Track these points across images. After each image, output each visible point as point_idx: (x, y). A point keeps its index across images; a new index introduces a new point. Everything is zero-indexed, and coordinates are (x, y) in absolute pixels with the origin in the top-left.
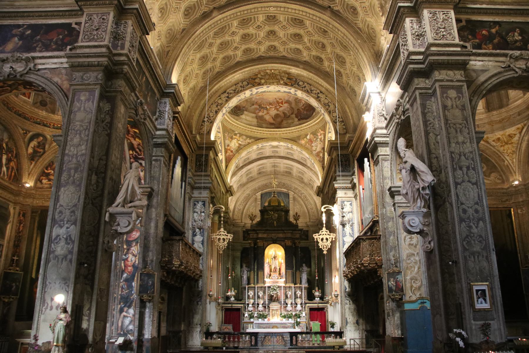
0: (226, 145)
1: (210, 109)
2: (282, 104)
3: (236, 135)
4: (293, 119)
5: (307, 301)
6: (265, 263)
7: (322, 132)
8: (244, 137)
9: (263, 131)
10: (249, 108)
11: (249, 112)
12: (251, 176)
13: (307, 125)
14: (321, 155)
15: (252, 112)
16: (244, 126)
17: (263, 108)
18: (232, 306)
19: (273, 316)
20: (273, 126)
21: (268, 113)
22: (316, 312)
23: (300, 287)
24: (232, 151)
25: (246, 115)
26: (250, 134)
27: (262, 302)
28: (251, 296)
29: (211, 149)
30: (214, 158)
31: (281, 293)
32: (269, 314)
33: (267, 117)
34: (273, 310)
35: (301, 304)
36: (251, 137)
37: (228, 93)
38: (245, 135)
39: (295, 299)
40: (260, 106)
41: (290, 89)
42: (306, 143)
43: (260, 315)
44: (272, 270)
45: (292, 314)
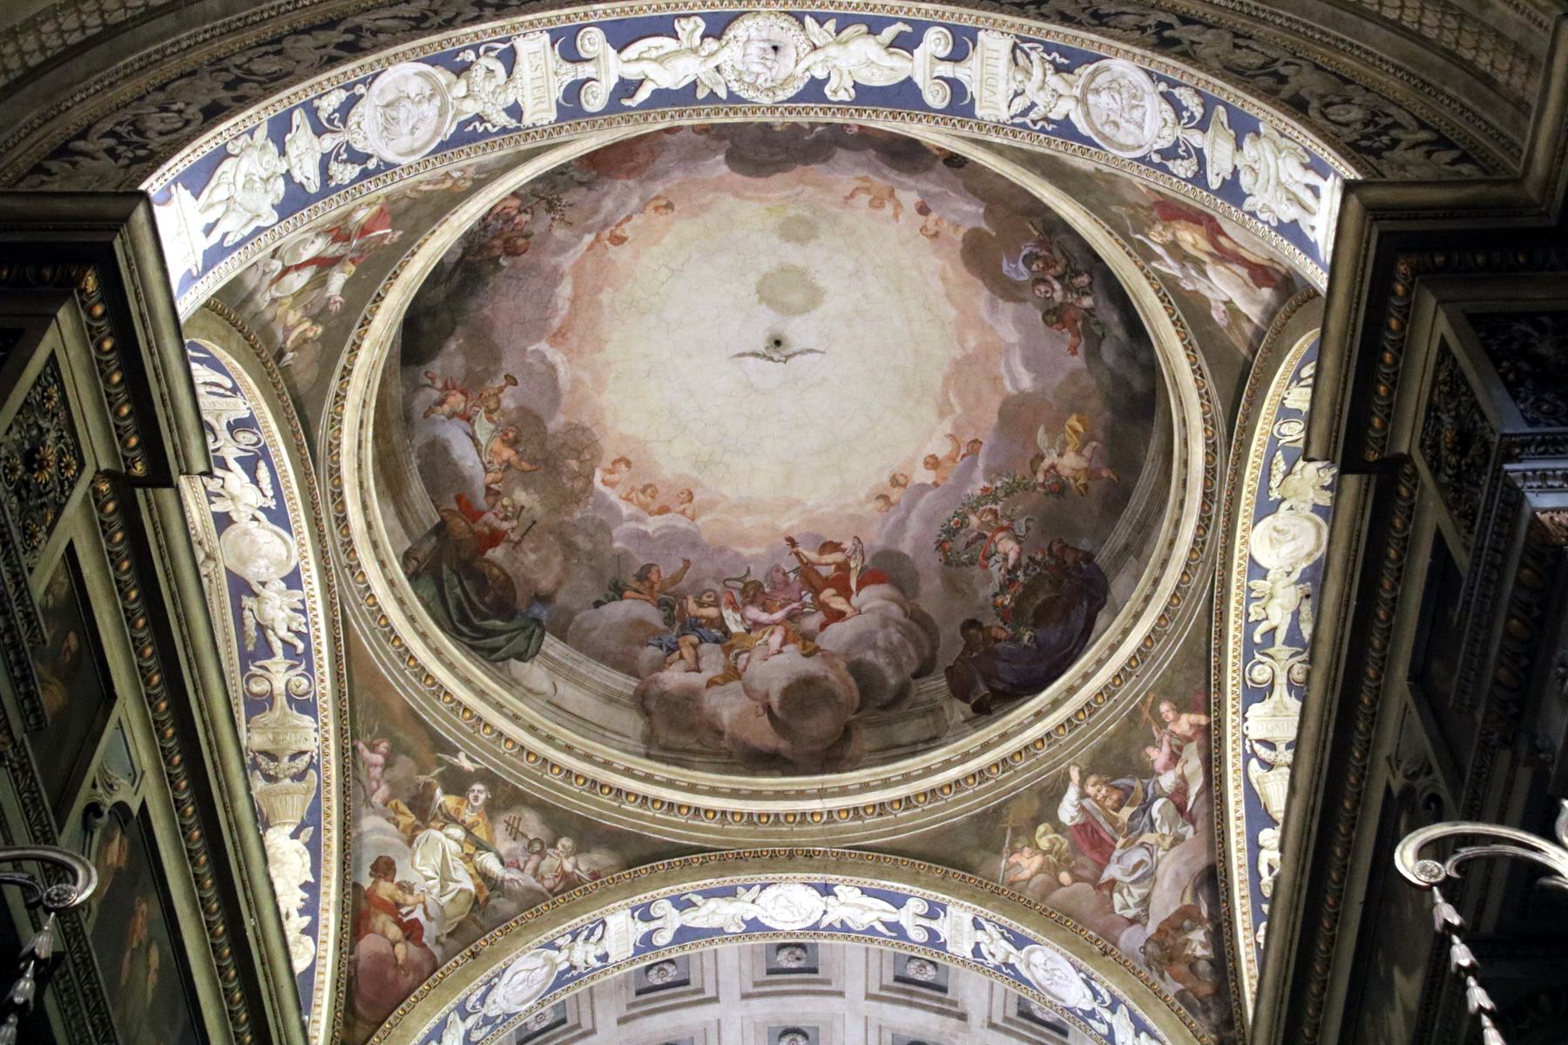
0: (368, 859)
1: (161, 97)
2: (845, 592)
3: (457, 783)
4: (935, 710)
7: (1185, 723)
8: (532, 824)
9: (692, 789)
10: (586, 617)
11: (581, 646)
13: (1055, 704)
14: (1197, 943)
15: (602, 657)
16: (532, 729)
17: (694, 625)
20: (778, 768)
21: (733, 674)
24: (412, 931)
25: (555, 667)
26: (576, 801)
29: (66, 288)
30: (123, 484)
33: (728, 707)
36: (587, 834)
37: (357, 30)
38: (540, 807)
40: (669, 606)
41: (907, 43)
42: (1051, 869)
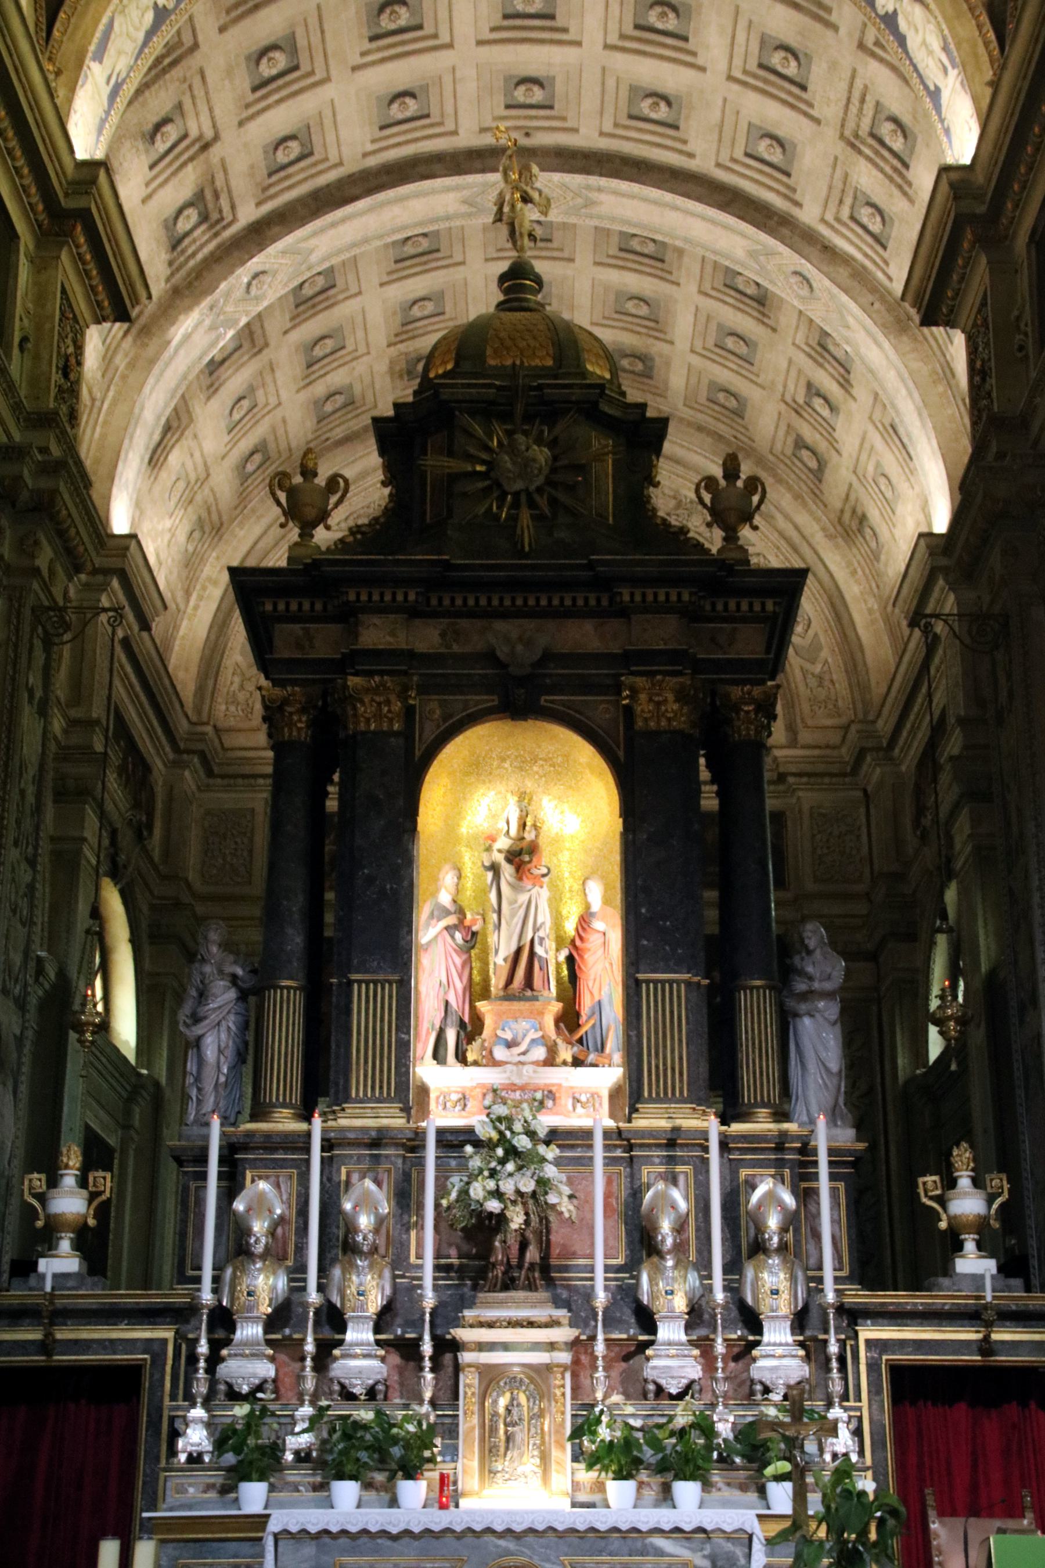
5: (858, 1297)
6: (422, 913)
12: (338, 378)
18: (46, 1347)
19: (490, 1452)
22: (961, 1412)
23: (781, 1143)
27: (375, 1302)
28: (259, 1227)
31: (580, 1197)
32: (451, 1431)
34: (491, 1377)
35: (800, 1320)
39: (733, 1267)
43: (352, 1429)
44: (496, 983)
45: (706, 1428)
